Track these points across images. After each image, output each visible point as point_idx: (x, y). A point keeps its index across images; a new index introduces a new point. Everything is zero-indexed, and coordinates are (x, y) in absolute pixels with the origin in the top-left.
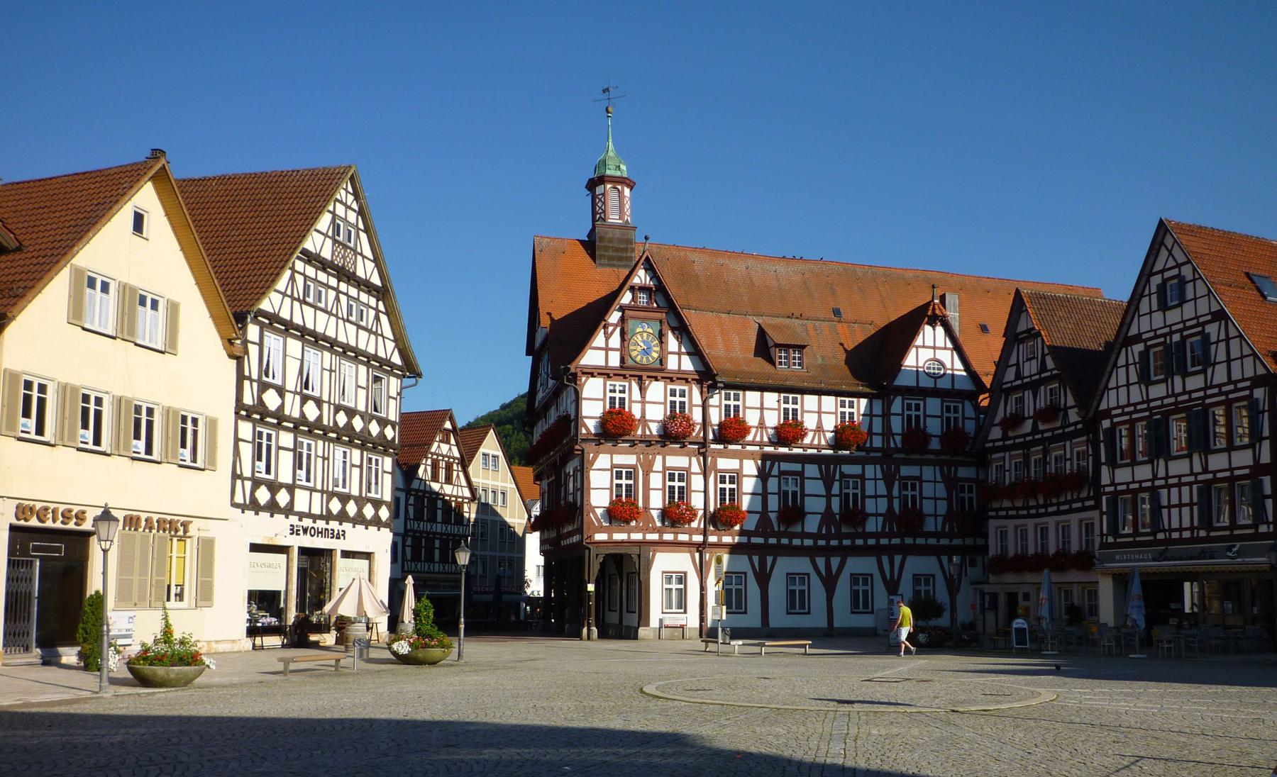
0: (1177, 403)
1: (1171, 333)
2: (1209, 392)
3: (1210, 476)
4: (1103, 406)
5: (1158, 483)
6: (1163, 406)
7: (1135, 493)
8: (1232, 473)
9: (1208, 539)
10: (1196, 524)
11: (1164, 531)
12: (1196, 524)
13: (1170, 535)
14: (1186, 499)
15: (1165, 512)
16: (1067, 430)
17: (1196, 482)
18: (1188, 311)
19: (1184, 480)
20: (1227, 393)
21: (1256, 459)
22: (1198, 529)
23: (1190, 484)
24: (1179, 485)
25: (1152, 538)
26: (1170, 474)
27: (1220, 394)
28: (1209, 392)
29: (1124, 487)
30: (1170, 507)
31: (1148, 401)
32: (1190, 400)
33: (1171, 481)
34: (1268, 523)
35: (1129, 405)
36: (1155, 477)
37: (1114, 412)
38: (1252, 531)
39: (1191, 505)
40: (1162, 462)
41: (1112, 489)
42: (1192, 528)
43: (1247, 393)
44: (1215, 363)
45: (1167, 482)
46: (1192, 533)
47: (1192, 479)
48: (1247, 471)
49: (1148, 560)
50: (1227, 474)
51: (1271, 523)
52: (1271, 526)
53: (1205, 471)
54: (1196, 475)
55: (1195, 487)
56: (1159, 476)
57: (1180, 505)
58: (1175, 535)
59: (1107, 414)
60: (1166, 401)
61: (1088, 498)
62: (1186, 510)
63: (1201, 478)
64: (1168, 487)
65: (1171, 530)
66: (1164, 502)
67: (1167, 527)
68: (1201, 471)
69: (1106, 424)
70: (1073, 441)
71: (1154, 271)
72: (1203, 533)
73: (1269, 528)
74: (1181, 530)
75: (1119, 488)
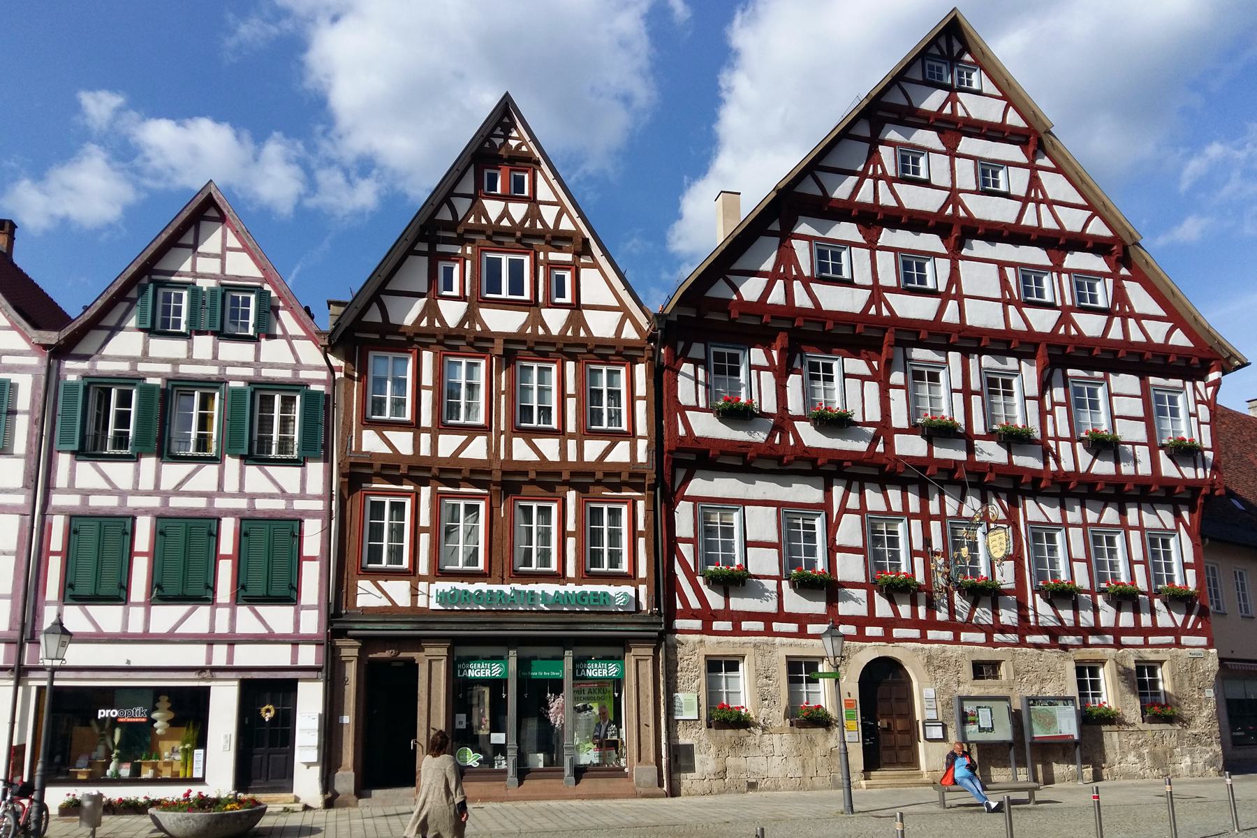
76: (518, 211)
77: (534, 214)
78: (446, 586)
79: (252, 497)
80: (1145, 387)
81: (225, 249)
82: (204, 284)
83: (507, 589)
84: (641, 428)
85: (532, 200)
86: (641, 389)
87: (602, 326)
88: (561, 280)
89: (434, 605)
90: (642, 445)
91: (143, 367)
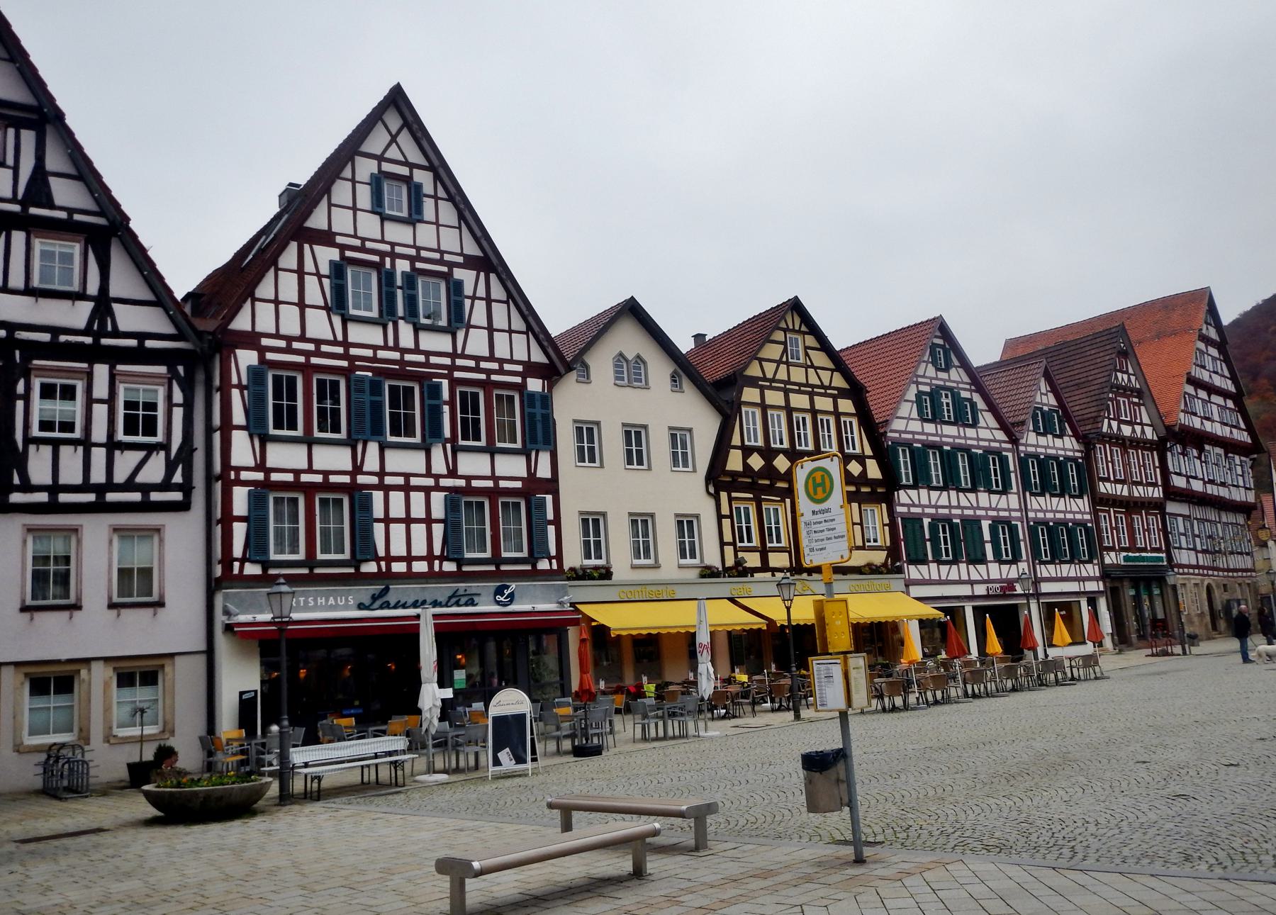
0: (401, 362)
1: (394, 256)
2: (459, 362)
3: (462, 483)
4: (241, 323)
5: (361, 479)
6: (374, 359)
7: (310, 489)
8: (496, 483)
9: (459, 576)
10: (437, 551)
11: (378, 559)
12: (437, 551)
13: (389, 567)
14: (418, 511)
15: (379, 529)
16: (105, 341)
17: (437, 488)
18: (426, 235)
19: (414, 481)
20: (489, 372)
21: (531, 474)
22: (442, 558)
23: (427, 490)
24: (407, 489)
25: (352, 570)
26: (388, 469)
27: (477, 369)
28: (459, 362)
29: (289, 477)
30: (387, 520)
31: (346, 344)
32: (427, 364)
33: (389, 480)
34: (550, 559)
35: (302, 338)
36: (357, 469)
37: (265, 342)
38: (528, 567)
39: (428, 521)
40: (373, 448)
41: (259, 476)
42: (430, 558)
43: (518, 380)
44: (469, 326)
45: (381, 480)
46: (431, 566)
47: (430, 482)
48: (518, 484)
49: (346, 607)
50: (490, 484)
51: (553, 557)
52: (554, 561)
53: (453, 473)
54: (437, 477)
55: (438, 498)
56: (365, 469)
57: (408, 521)
58: (399, 567)
59: (251, 340)
60: (382, 354)
61: (166, 486)
62: (419, 531)
63: (444, 482)
64: (387, 489)
65: (389, 559)
66: (378, 511)
67: (381, 553)
68: (445, 472)
69: (247, 358)
70: (120, 367)
71: (403, 160)
72: (449, 567)
73: (551, 564)
74: (409, 559)
75: (275, 477)
76: (1125, 377)
77: (1129, 380)
78: (1125, 554)
79: (1074, 513)
80: (1241, 461)
81: (1047, 391)
82: (1046, 408)
83: (1137, 554)
84: (1160, 483)
85: (1127, 372)
86: (1157, 464)
87: (1149, 434)
88: (1135, 410)
89: (1123, 563)
90: (1160, 488)
91: (1039, 450)
